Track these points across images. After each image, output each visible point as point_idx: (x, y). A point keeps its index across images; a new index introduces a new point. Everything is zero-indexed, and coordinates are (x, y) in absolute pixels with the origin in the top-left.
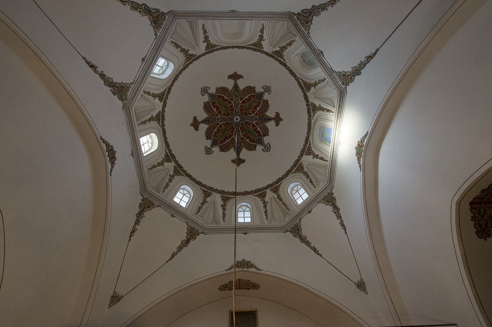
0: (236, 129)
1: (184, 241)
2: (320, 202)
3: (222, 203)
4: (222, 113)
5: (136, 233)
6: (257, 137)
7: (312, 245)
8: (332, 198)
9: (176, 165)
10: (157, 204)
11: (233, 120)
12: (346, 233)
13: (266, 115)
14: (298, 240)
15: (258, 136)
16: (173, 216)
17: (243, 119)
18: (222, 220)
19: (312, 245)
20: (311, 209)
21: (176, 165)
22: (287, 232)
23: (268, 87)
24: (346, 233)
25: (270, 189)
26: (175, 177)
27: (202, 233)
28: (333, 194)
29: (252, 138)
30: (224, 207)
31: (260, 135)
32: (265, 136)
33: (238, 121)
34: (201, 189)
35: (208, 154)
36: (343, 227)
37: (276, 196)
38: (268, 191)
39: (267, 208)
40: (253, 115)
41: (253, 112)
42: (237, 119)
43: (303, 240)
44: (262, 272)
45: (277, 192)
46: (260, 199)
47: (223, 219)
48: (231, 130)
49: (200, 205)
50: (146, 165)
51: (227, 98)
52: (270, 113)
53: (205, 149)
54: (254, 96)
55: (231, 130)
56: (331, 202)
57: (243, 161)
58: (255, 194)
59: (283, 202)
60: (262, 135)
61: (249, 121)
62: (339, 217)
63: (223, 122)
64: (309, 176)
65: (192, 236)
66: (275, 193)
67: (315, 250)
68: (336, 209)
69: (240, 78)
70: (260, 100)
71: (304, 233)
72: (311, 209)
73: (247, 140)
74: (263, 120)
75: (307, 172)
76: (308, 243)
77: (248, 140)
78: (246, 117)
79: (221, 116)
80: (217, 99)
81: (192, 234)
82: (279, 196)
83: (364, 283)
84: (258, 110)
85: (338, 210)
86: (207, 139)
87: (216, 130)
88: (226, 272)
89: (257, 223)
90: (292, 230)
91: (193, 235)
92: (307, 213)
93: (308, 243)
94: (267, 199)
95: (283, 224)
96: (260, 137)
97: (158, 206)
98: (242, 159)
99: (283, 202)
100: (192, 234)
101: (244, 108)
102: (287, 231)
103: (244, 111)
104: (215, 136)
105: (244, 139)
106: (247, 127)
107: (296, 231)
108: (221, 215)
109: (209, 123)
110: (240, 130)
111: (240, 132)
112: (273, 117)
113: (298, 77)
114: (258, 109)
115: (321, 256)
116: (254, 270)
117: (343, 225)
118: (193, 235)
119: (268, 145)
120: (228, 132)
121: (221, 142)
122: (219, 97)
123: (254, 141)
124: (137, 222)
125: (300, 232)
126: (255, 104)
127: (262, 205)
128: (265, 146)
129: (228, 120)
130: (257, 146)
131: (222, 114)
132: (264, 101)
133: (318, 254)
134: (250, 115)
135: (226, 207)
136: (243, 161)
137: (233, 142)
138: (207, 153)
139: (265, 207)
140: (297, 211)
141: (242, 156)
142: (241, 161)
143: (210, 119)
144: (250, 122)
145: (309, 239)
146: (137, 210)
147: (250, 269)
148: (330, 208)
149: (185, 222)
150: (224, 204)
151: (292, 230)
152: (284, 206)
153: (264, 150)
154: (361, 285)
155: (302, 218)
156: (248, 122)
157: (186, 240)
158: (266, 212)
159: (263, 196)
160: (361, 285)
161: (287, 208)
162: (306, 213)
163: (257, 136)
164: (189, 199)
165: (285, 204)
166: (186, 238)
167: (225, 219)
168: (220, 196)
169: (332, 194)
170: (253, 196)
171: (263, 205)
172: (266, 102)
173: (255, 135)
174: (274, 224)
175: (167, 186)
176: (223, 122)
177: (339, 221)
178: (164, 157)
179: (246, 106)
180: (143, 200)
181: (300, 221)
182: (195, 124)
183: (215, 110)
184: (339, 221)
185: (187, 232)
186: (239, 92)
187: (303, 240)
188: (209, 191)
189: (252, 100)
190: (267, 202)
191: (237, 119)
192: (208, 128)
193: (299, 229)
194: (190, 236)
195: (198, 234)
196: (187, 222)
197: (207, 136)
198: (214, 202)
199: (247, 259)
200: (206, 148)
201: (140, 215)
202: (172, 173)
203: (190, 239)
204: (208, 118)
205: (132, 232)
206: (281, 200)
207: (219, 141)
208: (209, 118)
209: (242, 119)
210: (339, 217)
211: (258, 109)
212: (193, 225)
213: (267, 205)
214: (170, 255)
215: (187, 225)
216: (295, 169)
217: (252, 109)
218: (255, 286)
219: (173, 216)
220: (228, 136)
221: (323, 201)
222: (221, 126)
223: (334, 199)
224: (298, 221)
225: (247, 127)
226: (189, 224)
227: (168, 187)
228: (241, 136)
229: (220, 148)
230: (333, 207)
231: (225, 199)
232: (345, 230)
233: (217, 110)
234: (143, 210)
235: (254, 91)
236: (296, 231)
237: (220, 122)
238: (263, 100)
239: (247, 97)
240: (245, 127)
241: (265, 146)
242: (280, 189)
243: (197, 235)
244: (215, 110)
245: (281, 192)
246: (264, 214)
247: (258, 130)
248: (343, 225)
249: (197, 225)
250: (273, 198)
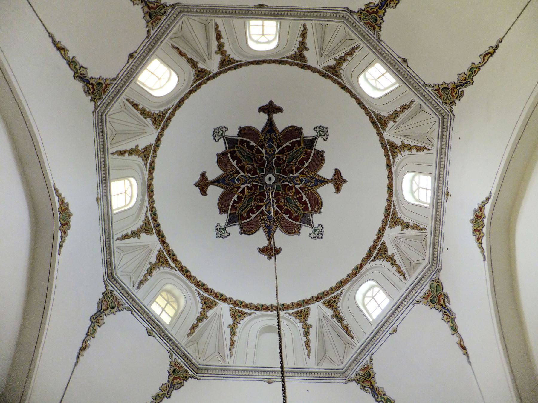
0: (272, 163)
1: (391, 5)
2: (114, 79)
4: (293, 191)
5: (484, 49)
6: (236, 149)
8: (92, 93)
9: (381, 130)
10: (429, 89)
11: (276, 179)
12: (51, 36)
13: (223, 188)
15: (235, 151)
17: (260, 179)
20: (130, 62)
21: (381, 130)
22: (173, 5)
23: (220, 237)
24: (51, 36)
25: (212, 74)
26: (386, 115)
27: (351, 12)
28: (91, 100)
29: (246, 148)
31: (233, 154)
32: (223, 154)
33: (268, 182)
35: (324, 128)
36: (59, 45)
37: (200, 65)
39: (216, 43)
40: (243, 187)
41: (243, 192)
42: (270, 179)
45: (199, 72)
46: (230, 57)
48: (281, 162)
50: (431, 156)
51: (285, 216)
52: (215, 192)
53: (327, 135)
54: (243, 218)
55: (281, 162)
56: (93, 84)
57: (261, 109)
60: (229, 155)
61: (250, 176)
62: (72, 63)
63: (293, 175)
64: (141, 114)
65: (373, 12)
68: (80, 76)
69: (264, 248)
70: (232, 212)
72: (130, 62)
73: (254, 145)
74: (226, 179)
75: (146, 118)
77: (252, 144)
78: (254, 183)
79: (296, 186)
80: (300, 215)
84: (236, 196)
85: (76, 75)
86: (322, 151)
87: (306, 164)
89: (237, 22)
90: (163, 11)
91: (370, 13)
92: (136, 52)
94: (218, 58)
96: (231, 150)
97: (429, 85)
98: (265, 113)
101: (258, 197)
102: (173, 6)
103: (257, 193)
104: (308, 154)
105: (260, 146)
106: (253, 165)
109: (317, 177)
110: (265, 161)
111: (266, 157)
112: (211, 186)
113: (177, 269)
114: (235, 198)
117: (61, 49)
118: (370, 13)
119: (217, 138)
120: (286, 158)
121: (299, 143)
122: (296, 219)
123: (242, 142)
124: (474, 70)
125: (146, 9)
126: (241, 204)
128: (222, 136)
129: (285, 178)
130: (236, 135)
131: (294, 189)
132: (226, 212)
134: (249, 185)
136: (261, 109)
137: (278, 141)
138: (325, 130)
141: (264, 117)
142: (266, 109)
143: (313, 183)
144: (249, 174)
146: (468, 90)
148: (93, 73)
149: (382, 43)
151: (163, 11)
153: (224, 129)
155: (147, 40)
156: (252, 175)
157: (387, 6)
158: (219, 37)
159: (226, 63)
161: (177, 48)
162: (138, 51)
163: (237, 152)
166: (386, 11)
169: (93, 100)
171: (225, 49)
172: (223, 209)
173: (243, 210)
175: (404, 108)
176: (293, 175)
178: (399, 154)
179: (255, 201)
180: (453, 103)
181: (148, 32)
182: (338, 181)
183: (305, 198)
184: (70, 55)
185: (382, 21)
186: (265, 224)
189: (246, 211)
190: (218, 53)
191: (270, 179)
192: (318, 170)
193: (150, 16)
194: (377, 12)
195: (360, 12)
196: (380, 41)
197: (322, 156)
198: (321, 55)
200: (325, 137)
201: (466, 81)
202: (391, 124)
203: (377, 7)
204: (317, 185)
205: (491, 54)
207: (302, 145)
208: (315, 185)
209: (261, 179)
210: (72, 63)
211: (235, 198)
212: (369, 32)
213: (216, 49)
215: (379, 36)
217: (246, 196)
219: (405, 60)
220: (287, 153)
221: (108, 82)
222: (298, 169)
223: (87, 93)
224: (152, 32)
225: (253, 165)
226: (375, 36)
227: (403, 106)
228: (263, 151)
229: (301, 133)
230: (87, 78)
232: (54, 41)
233: (302, 197)
234: (457, 87)
235: (241, 228)
237: (298, 177)
238: (228, 213)
239: (253, 216)
240: (257, 166)
241: (222, 136)
243: (364, 10)
244: (305, 198)
246: (223, 34)
247: (235, 161)
248: (61, 49)
249: (359, 29)
250: (207, 59)
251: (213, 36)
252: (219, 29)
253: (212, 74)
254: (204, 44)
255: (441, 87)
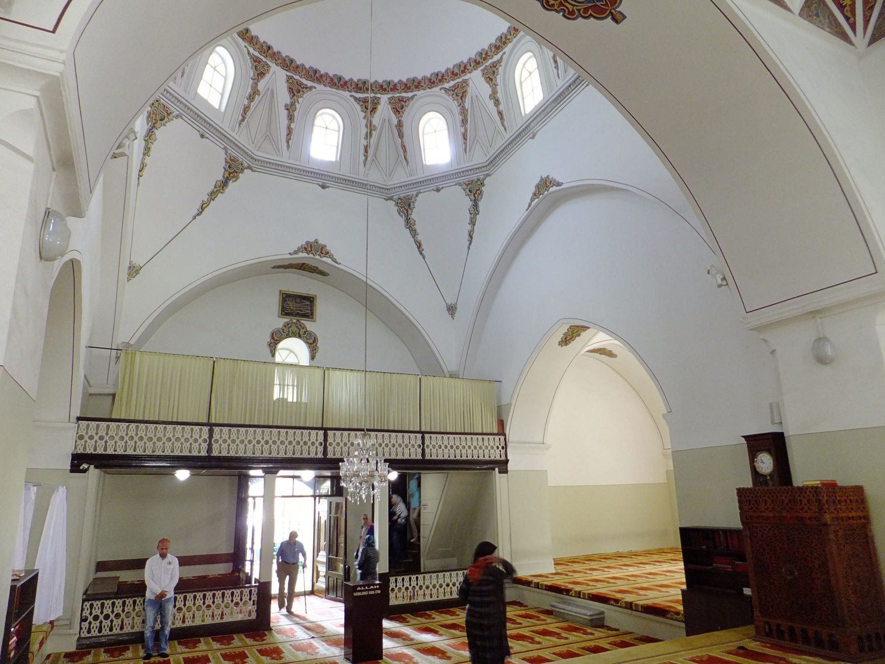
2: (460, 184)
3: (288, 101)
7: (419, 238)
10: (176, 113)
12: (469, 248)
14: (401, 221)
16: (202, 136)
18: (285, 144)
19: (419, 238)
24: (469, 248)
27: (249, 168)
30: (290, 109)
34: (249, 53)
37: (395, 121)
38: (384, 98)
43: (410, 224)
44: (340, 266)
47: (288, 142)
49: (246, 102)
58: (358, 95)
59: (402, 142)
62: (473, 222)
66: (395, 114)
67: (419, 246)
68: (475, 209)
71: (414, 215)
76: (414, 233)
81: (233, 169)
82: (400, 125)
83: (456, 308)
88: (289, 256)
89: (345, 171)
91: (235, 171)
93: (414, 233)
94: (376, 120)
95: (390, 183)
97: (177, 116)
99: (402, 142)
100: (233, 169)
102: (391, 199)
107: (405, 206)
108: (284, 132)
115: (424, 257)
116: (329, 261)
127: (364, 130)
133: (421, 254)
135: (296, 113)
139: (369, 135)
140: (420, 176)
145: (417, 227)
147: (324, 259)
148: (468, 203)
150: (293, 104)
152: (401, 151)
154: (452, 310)
160: (452, 310)
161: (406, 159)
164: (223, 79)
165: (405, 146)
167: (290, 142)
168: (284, 78)
169: (482, 184)
170: (352, 99)
174: (374, 177)
177: (469, 227)
181: (417, 196)
184: (469, 227)
187: (410, 224)
188: (264, 60)
193: (409, 205)
194: (230, 173)
196: (225, 149)
198: (272, 91)
199: (322, 242)
206: (401, 135)
210: (473, 222)
213: (374, 132)
214: (198, 206)
215: (226, 153)
216: (452, 83)
218: (322, 273)
221: (465, 187)
224: (415, 193)
231: (296, 89)
232: (470, 244)
234: (153, 127)
236: (405, 206)
242: (407, 109)
245: (406, 117)
248: (471, 237)
251: (371, 151)
252: (364, 158)
253: (389, 96)
254: (383, 135)
255: (166, 119)
